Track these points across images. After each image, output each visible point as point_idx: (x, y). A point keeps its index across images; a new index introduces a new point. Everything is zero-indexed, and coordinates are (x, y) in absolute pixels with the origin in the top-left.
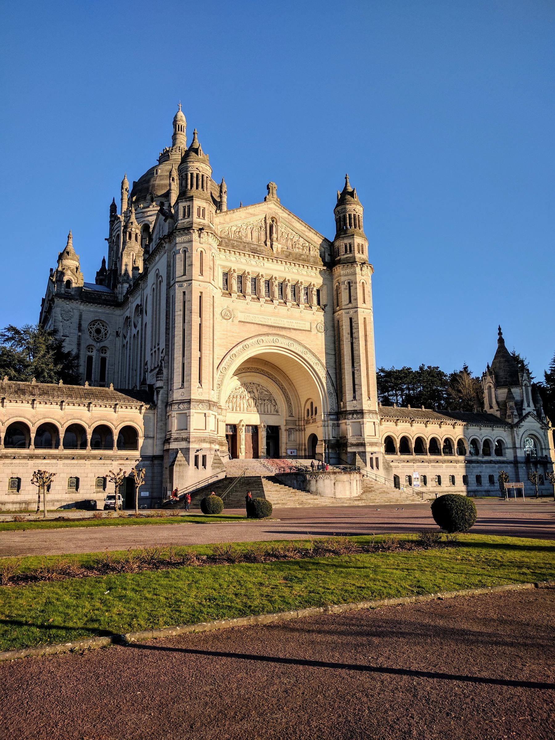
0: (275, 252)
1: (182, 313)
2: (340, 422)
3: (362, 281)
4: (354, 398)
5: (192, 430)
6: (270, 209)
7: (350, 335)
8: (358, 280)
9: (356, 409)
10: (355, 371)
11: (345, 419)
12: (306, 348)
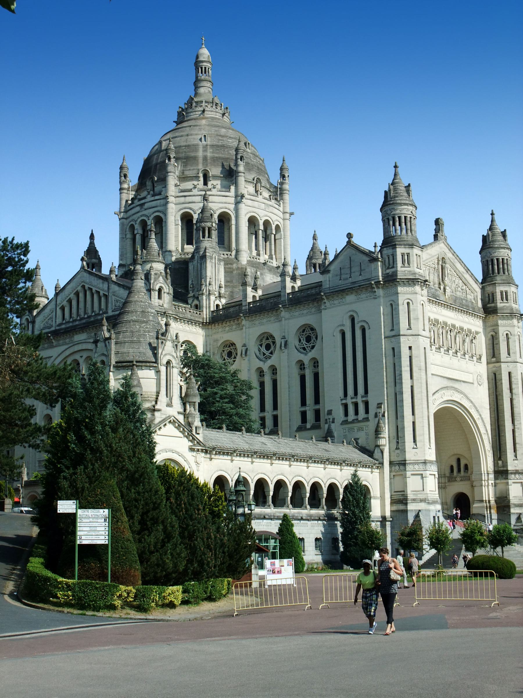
0: (447, 297)
1: (409, 369)
2: (497, 481)
3: (519, 333)
4: (516, 456)
5: (428, 492)
6: (441, 248)
7: (509, 391)
8: (516, 333)
9: (517, 469)
10: (516, 430)
11: (508, 479)
12: (472, 402)
